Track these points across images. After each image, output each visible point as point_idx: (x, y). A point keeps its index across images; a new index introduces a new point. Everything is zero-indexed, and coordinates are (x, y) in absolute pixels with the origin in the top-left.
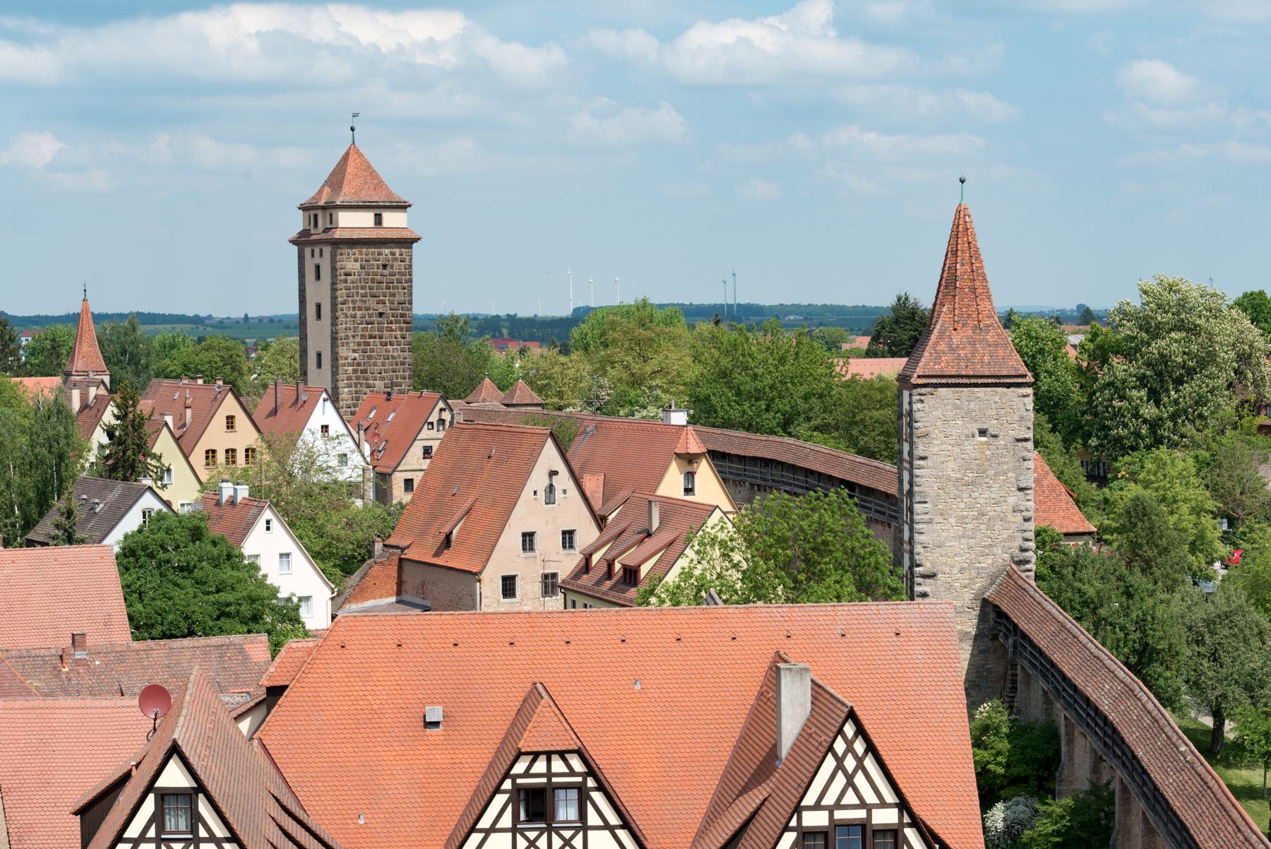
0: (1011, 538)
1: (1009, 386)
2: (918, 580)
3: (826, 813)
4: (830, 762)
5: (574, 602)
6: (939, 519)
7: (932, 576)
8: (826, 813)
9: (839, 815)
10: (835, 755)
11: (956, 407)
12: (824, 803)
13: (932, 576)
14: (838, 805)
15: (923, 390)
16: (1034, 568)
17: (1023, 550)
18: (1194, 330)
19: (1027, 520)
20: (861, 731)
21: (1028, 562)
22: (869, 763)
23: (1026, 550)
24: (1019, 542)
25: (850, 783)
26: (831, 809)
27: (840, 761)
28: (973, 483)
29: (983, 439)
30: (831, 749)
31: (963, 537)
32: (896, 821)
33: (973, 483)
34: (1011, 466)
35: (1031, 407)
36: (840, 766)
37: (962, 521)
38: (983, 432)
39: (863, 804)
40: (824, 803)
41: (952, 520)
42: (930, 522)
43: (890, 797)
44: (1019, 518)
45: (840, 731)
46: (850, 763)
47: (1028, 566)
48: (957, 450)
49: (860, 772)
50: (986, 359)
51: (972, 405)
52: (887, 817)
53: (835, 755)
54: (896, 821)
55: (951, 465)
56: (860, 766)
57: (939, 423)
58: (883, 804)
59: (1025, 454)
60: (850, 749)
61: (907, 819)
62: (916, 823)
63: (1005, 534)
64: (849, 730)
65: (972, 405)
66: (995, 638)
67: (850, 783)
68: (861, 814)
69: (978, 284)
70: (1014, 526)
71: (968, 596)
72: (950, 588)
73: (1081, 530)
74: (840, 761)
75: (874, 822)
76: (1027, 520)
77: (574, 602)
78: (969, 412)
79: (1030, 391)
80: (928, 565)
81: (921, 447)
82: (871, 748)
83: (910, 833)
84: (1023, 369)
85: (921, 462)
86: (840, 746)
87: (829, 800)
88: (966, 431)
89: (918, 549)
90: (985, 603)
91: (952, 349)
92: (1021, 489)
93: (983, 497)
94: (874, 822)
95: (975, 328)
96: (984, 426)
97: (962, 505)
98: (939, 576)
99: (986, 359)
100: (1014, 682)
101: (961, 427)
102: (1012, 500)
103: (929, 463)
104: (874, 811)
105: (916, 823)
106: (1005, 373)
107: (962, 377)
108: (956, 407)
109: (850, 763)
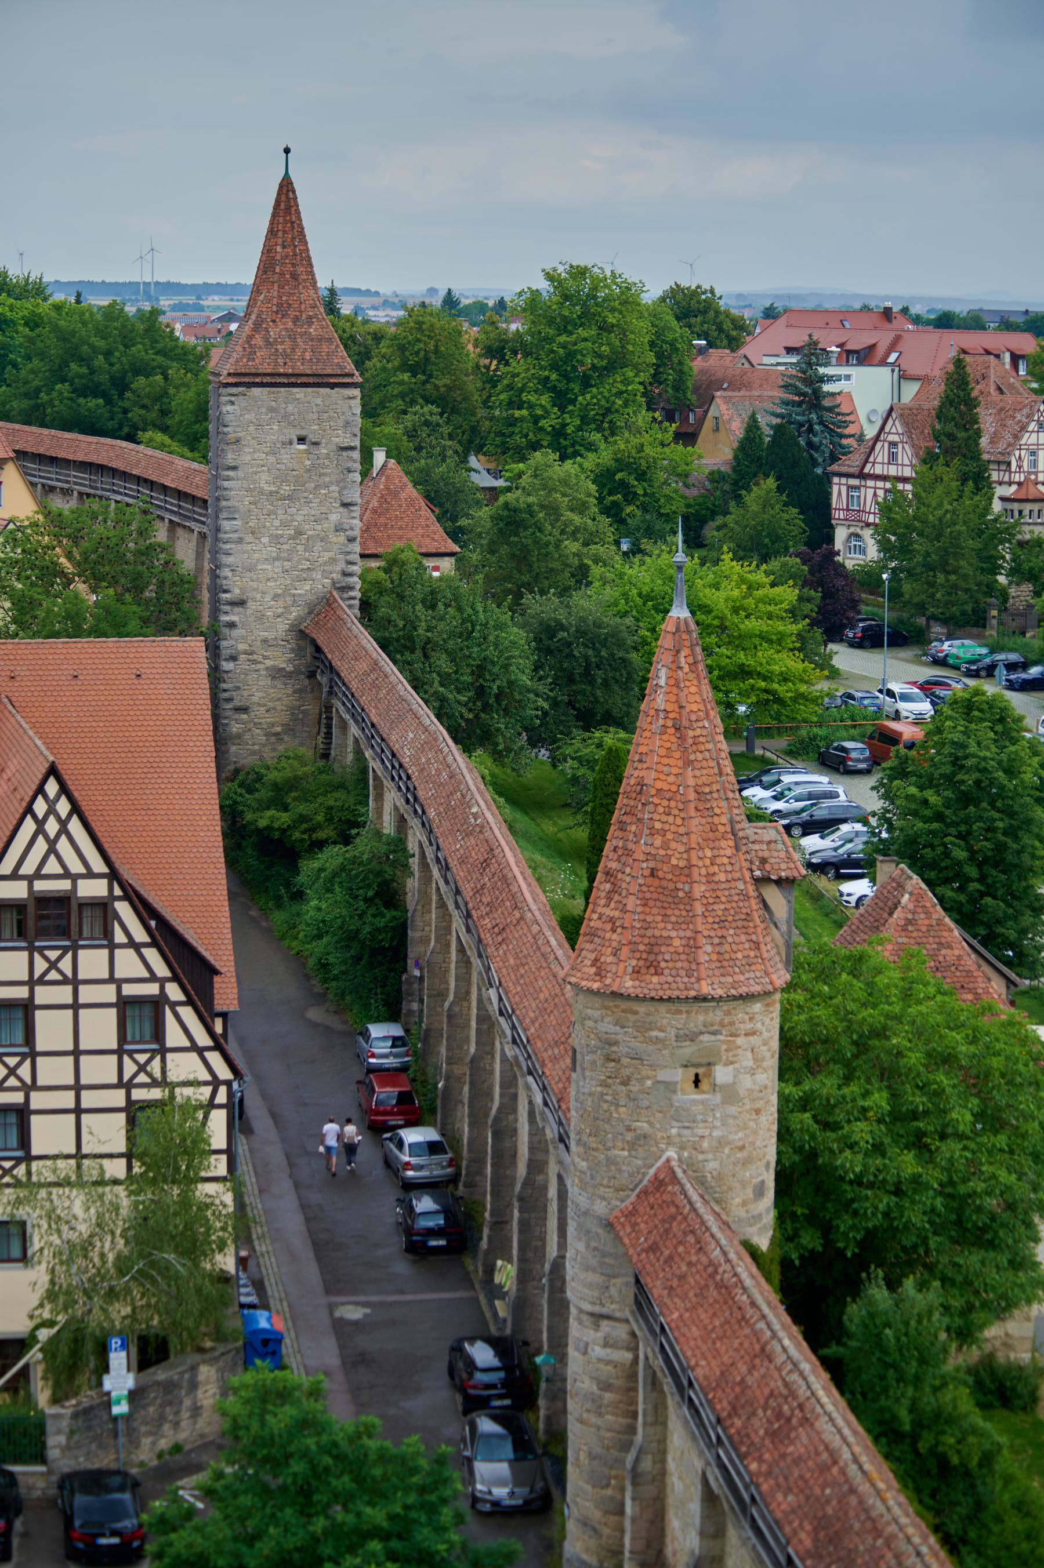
0: (333, 561)
1: (333, 386)
2: (227, 608)
3: (25, 883)
4: (29, 826)
5: (809, 600)
6: (249, 538)
7: (241, 603)
8: (25, 883)
9: (39, 886)
10: (34, 817)
11: (272, 410)
12: (21, 872)
13: (241, 603)
14: (38, 875)
15: (234, 390)
16: (359, 595)
17: (345, 574)
18: (605, 328)
19: (351, 540)
20: (64, 789)
21: (351, 588)
22: (75, 826)
23: (350, 575)
24: (341, 566)
25: (52, 850)
26: (30, 879)
27: (40, 824)
28: (289, 498)
29: (302, 447)
30: (29, 810)
31: (277, 559)
32: (105, 893)
33: (289, 498)
34: (334, 478)
35: (358, 410)
36: (40, 830)
37: (276, 539)
38: (301, 440)
39: (67, 874)
40: (21, 872)
41: (265, 540)
42: (240, 541)
43: (98, 865)
44: (342, 538)
45: (40, 790)
46: (52, 827)
47: (352, 594)
48: (272, 459)
49: (63, 837)
50: (308, 356)
51: (290, 408)
52: (94, 889)
53: (34, 817)
54: (105, 893)
55: (264, 477)
56: (63, 830)
57: (252, 428)
58: (90, 875)
59: (350, 464)
60: (51, 811)
61: (118, 892)
62: (132, 896)
63: (326, 556)
64: (52, 788)
65: (290, 408)
66: (312, 675)
67: (52, 849)
68: (65, 885)
69: (301, 269)
70: (336, 548)
71: (282, 627)
72: (260, 618)
73: (443, 550)
74: (40, 824)
75: (80, 894)
76: (351, 540)
77: (809, 600)
78: (286, 416)
79: (357, 392)
80: (237, 591)
81: (230, 456)
82: (76, 809)
83: (123, 909)
84: (350, 366)
85: (231, 473)
86: (40, 807)
87: (28, 868)
88: (282, 438)
89: (226, 572)
90: (302, 635)
91: (268, 344)
92: (345, 505)
93: (300, 514)
94: (80, 894)
95: (296, 320)
96: (303, 433)
97: (277, 523)
98: (250, 604)
99: (308, 356)
100: (329, 726)
101: (275, 432)
102: (334, 517)
103: (240, 474)
104: (80, 882)
105: (132, 896)
106: (329, 371)
107: (280, 375)
108: (272, 410)
109: (52, 827)
